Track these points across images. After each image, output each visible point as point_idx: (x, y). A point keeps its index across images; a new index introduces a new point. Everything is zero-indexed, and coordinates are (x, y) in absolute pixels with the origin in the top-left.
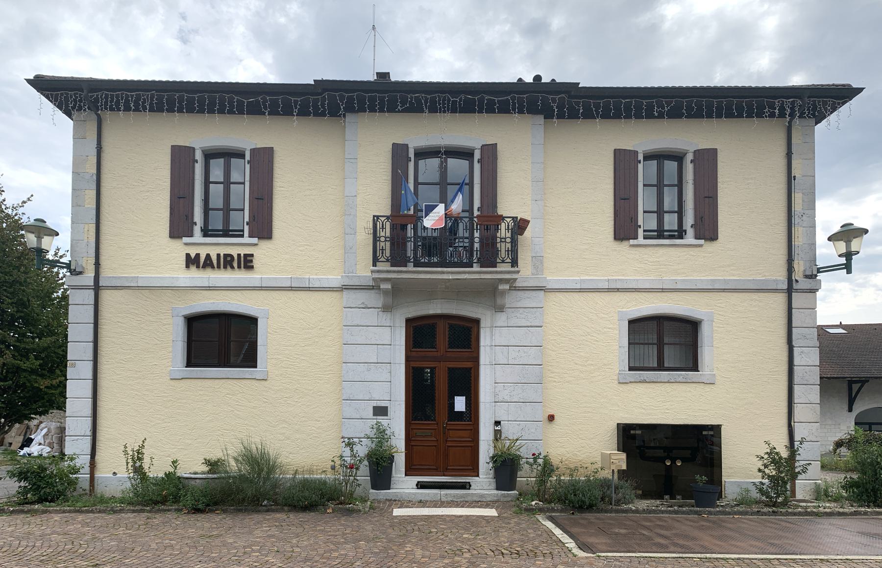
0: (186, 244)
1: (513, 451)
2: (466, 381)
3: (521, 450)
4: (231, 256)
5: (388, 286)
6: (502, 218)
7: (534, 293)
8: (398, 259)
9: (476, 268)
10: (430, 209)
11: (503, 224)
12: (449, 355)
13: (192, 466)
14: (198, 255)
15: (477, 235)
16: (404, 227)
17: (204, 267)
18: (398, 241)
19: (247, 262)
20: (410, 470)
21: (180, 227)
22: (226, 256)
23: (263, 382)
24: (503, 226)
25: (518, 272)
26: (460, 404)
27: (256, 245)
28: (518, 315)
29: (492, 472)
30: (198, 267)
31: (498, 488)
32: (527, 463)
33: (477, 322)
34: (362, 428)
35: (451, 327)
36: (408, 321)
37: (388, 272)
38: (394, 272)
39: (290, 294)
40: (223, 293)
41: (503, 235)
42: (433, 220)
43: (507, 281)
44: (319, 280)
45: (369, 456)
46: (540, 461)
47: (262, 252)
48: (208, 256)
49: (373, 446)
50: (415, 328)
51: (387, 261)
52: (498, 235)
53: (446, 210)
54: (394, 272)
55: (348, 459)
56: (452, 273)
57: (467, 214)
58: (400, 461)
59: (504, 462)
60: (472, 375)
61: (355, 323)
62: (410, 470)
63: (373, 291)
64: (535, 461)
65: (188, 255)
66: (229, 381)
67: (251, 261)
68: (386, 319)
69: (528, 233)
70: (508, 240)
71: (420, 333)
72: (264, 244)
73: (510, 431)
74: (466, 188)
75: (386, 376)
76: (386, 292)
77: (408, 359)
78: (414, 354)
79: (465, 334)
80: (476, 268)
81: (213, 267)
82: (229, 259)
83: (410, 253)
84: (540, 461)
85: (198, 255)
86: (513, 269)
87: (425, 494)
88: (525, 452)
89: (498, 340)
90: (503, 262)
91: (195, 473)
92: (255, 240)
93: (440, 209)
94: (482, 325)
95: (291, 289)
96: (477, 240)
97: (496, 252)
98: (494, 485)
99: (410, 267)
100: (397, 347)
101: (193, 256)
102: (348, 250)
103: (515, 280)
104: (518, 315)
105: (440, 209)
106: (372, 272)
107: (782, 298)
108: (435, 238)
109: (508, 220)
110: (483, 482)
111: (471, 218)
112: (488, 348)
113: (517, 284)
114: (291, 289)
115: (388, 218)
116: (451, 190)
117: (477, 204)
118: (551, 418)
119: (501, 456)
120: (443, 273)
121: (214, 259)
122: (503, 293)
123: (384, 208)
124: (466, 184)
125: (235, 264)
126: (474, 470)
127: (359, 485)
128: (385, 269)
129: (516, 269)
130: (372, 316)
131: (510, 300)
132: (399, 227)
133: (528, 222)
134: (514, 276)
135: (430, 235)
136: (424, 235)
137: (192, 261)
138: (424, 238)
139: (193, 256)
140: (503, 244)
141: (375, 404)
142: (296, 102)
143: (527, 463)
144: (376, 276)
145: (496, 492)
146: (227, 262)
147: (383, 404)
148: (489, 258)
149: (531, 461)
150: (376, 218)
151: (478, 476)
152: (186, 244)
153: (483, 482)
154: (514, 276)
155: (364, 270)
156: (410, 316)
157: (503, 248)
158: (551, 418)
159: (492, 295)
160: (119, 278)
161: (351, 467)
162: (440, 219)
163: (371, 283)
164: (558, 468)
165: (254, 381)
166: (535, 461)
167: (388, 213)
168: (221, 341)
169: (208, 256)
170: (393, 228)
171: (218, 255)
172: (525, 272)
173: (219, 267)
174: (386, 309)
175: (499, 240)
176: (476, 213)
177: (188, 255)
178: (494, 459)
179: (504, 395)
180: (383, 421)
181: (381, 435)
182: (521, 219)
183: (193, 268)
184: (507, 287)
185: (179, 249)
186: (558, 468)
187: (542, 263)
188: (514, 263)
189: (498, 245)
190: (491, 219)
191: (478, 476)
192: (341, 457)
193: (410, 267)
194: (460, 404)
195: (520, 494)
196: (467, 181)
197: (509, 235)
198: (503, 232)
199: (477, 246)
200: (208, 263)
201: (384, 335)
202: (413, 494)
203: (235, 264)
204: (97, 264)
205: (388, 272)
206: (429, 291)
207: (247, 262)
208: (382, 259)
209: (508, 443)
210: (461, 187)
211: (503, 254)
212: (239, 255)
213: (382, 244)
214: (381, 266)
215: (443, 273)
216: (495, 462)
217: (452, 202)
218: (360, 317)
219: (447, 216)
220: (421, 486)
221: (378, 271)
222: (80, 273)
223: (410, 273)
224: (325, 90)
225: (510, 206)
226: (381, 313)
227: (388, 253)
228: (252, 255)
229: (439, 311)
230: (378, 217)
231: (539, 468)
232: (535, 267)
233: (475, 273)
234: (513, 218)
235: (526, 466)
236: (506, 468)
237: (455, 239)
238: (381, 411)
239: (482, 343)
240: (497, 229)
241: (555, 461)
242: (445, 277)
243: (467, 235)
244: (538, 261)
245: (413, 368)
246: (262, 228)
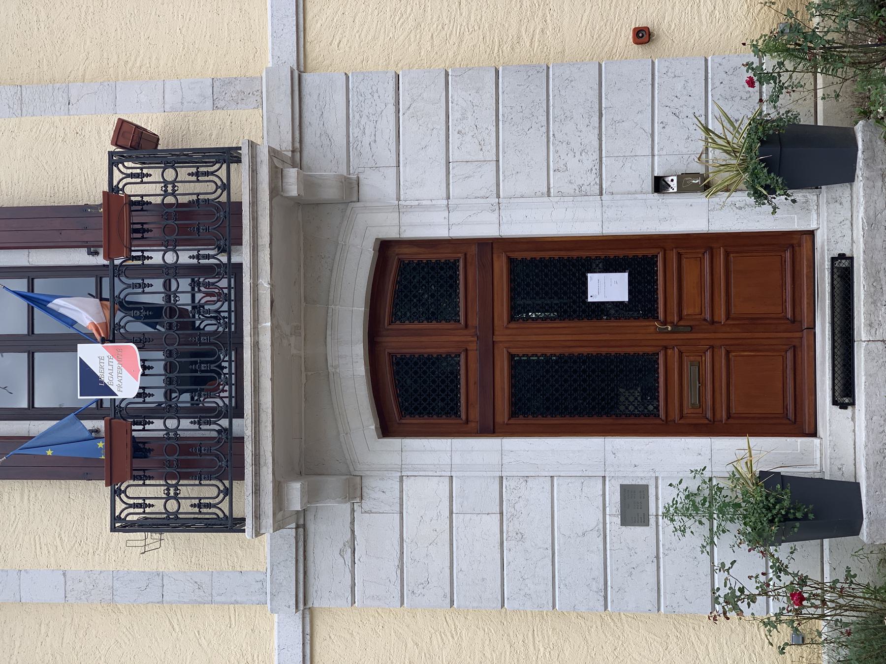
1: (738, 140)
2: (547, 271)
3: (734, 114)
5: (295, 491)
6: (112, 193)
7: (310, 101)
8: (221, 460)
9: (243, 256)
10: (90, 381)
11: (129, 190)
12: (474, 321)
15: (156, 258)
16: (140, 449)
18: (182, 461)
20: (802, 424)
24: (133, 190)
25: (252, 145)
28: (367, 140)
29: (799, 195)
31: (848, 177)
32: (774, 99)
33: (385, 248)
34: (689, 560)
35: (396, 317)
36: (386, 429)
37: (257, 491)
38: (257, 474)
41: (158, 189)
42: (123, 374)
43: (277, 175)
45: (759, 539)
46: (769, 63)
49: (735, 527)
50: (407, 410)
51: (228, 492)
52: (158, 200)
53: (89, 338)
54: (257, 474)
56: (256, 320)
57: (106, 282)
58: (774, 452)
59: (771, 165)
60: (528, 255)
62: (802, 424)
63: (311, 527)
64: (769, 77)
68: (381, 491)
69: (151, 123)
70: (170, 174)
71: (418, 397)
73: (680, 152)
74: (42, 286)
75: (537, 492)
76: (312, 495)
77: (489, 429)
78: (475, 414)
79: (417, 279)
80: (243, 256)
83: (210, 431)
84: (769, 63)
86: (245, 159)
88: (743, 107)
89: (433, 189)
90: (226, 187)
93: (92, 354)
94: (392, 234)
96: (170, 258)
97: (198, 205)
98: (840, 190)
99: (243, 426)
100: (457, 460)
102: (205, 594)
103: (274, 153)
104: (367, 140)
105: (92, 354)
106: (258, 533)
108: (169, 367)
109: (117, 176)
110: (829, 220)
111: (117, 272)
112: (455, 217)
113: (285, 144)
115: (116, 493)
116: (44, 325)
117: (79, 257)
118: (643, 36)
119: (754, 175)
120: (256, 346)
122: (308, 183)
123: (86, 503)
124: (31, 287)
126: (798, 243)
128: (249, 499)
129: (245, 153)
130: (375, 528)
131: (327, 164)
132: (139, 463)
133: (122, 123)
134: (264, 156)
135: (160, 381)
136: (159, 396)
138: (168, 395)
140: (181, 188)
143: (774, 99)
144: (268, 521)
145: (859, 184)
148: (217, 223)
149: (767, 89)
150: (119, 525)
151: (811, 233)
153: (829, 220)
154: (264, 156)
155: (257, 552)
156: (374, 433)
157: (190, 187)
158: (643, 36)
159: (312, 213)
162: (116, 355)
163: (289, 532)
166: (769, 77)
167: (100, 490)
170: (142, 476)
172: (253, 126)
174: (354, 490)
175: (170, 200)
176: (100, 260)
178: (762, 193)
179: (580, 169)
180: (662, 497)
181: (703, 504)
182: (115, 142)
184: (292, 174)
187: (229, 82)
188: (229, 156)
189: (183, 200)
190: (117, 222)
191: (811, 233)
193: (243, 426)
194: (608, 287)
196: (21, 285)
197: (156, 174)
198: (148, 187)
199: (185, 257)
201: (425, 496)
205: (257, 491)
206: (304, 380)
208: (225, 506)
209: (716, 155)
210: (36, 302)
211: (206, 188)
213: (186, 506)
214: (243, 506)
215: (256, 346)
216: (772, 191)
217: (71, 323)
219: (111, 335)
220: (845, 395)
221: (257, 517)
223: (259, 427)
225: (80, 172)
226: (367, 504)
227: (208, 491)
230: (115, 519)
231: (789, 65)
232: (240, 99)
233: (257, 257)
234: (112, 164)
235: (784, 100)
236: (787, 156)
237: (172, 311)
239: (441, 232)
240: (142, 205)
241: (767, 23)
242: (266, 340)
243: (158, 284)
244: (224, 91)
245: (513, 414)
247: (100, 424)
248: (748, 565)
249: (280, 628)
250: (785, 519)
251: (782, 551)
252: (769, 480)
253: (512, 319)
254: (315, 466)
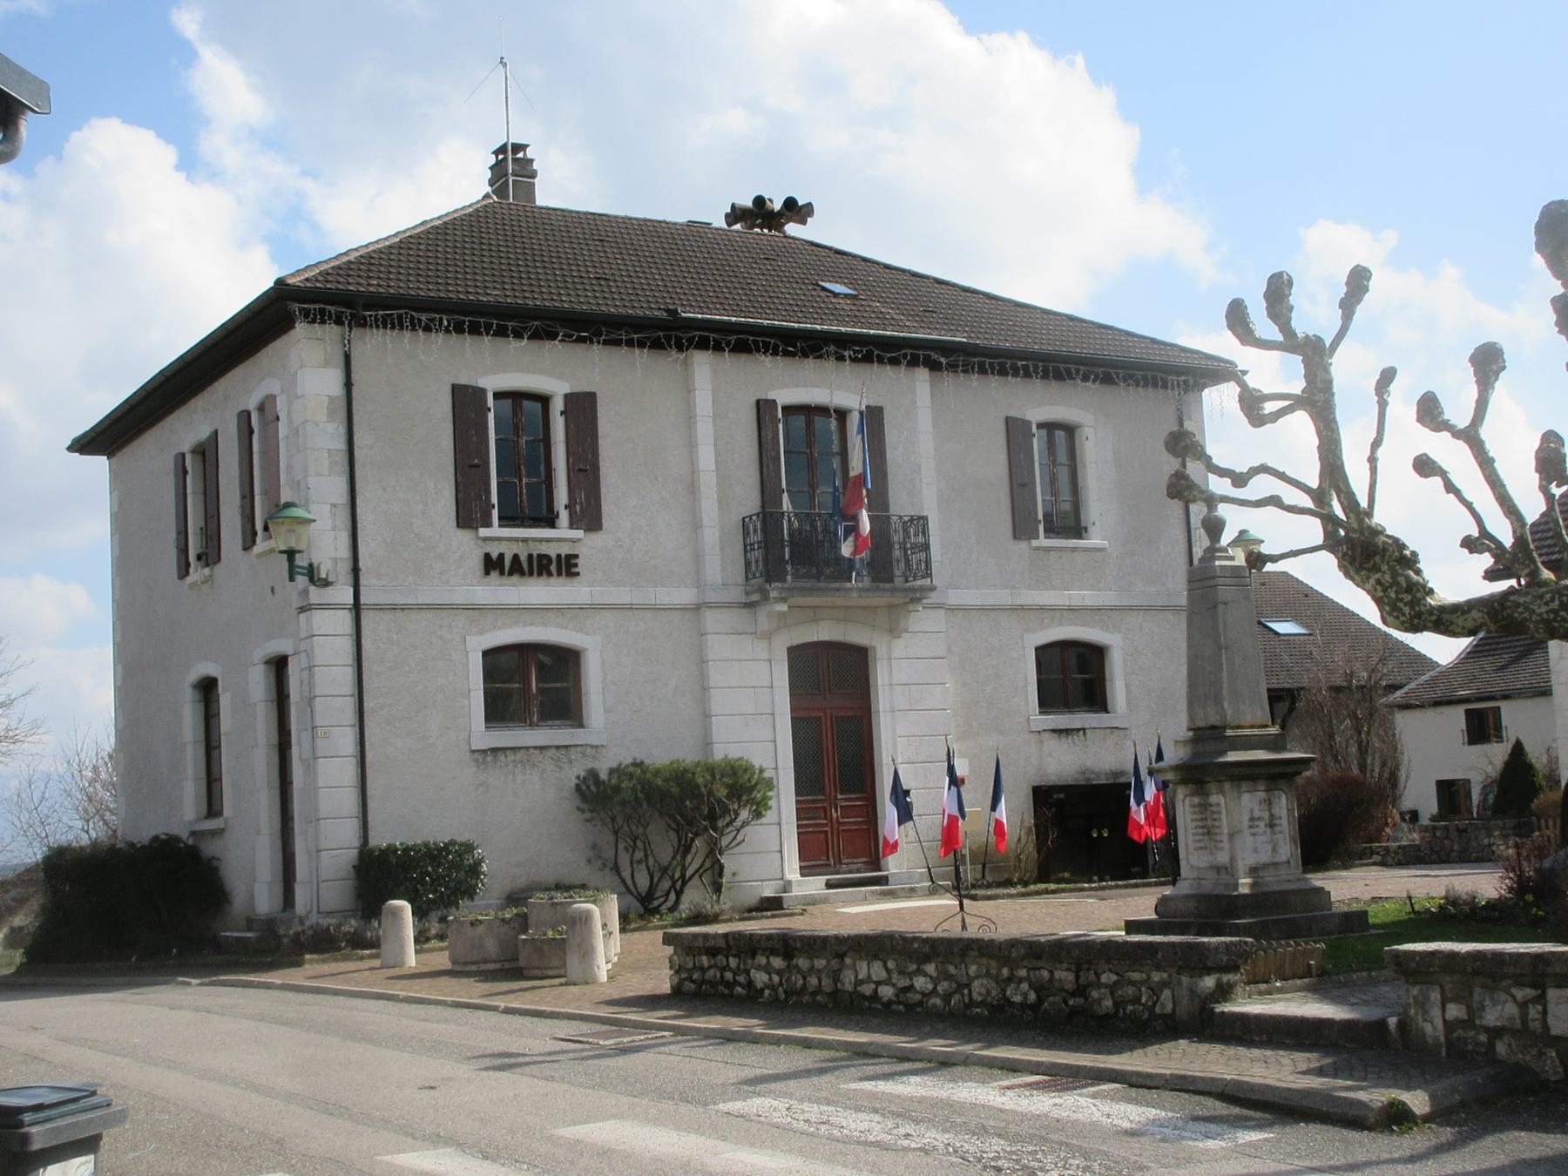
4: (548, 557)
14: (501, 556)
17: (511, 574)
19: (567, 566)
21: (469, 514)
22: (540, 557)
30: (502, 573)
36: (792, 651)
40: (533, 612)
47: (588, 546)
48: (516, 557)
65: (487, 556)
67: (576, 565)
72: (595, 539)
81: (522, 574)
85: (501, 556)
92: (579, 534)
101: (494, 555)
121: (523, 558)
125: (553, 568)
137: (492, 565)
139: (494, 555)
146: (541, 566)
169: (516, 557)
173: (531, 574)
177: (487, 556)
183: (494, 574)
185: (467, 547)
203: (553, 568)
228: (576, 556)
246: (589, 516)
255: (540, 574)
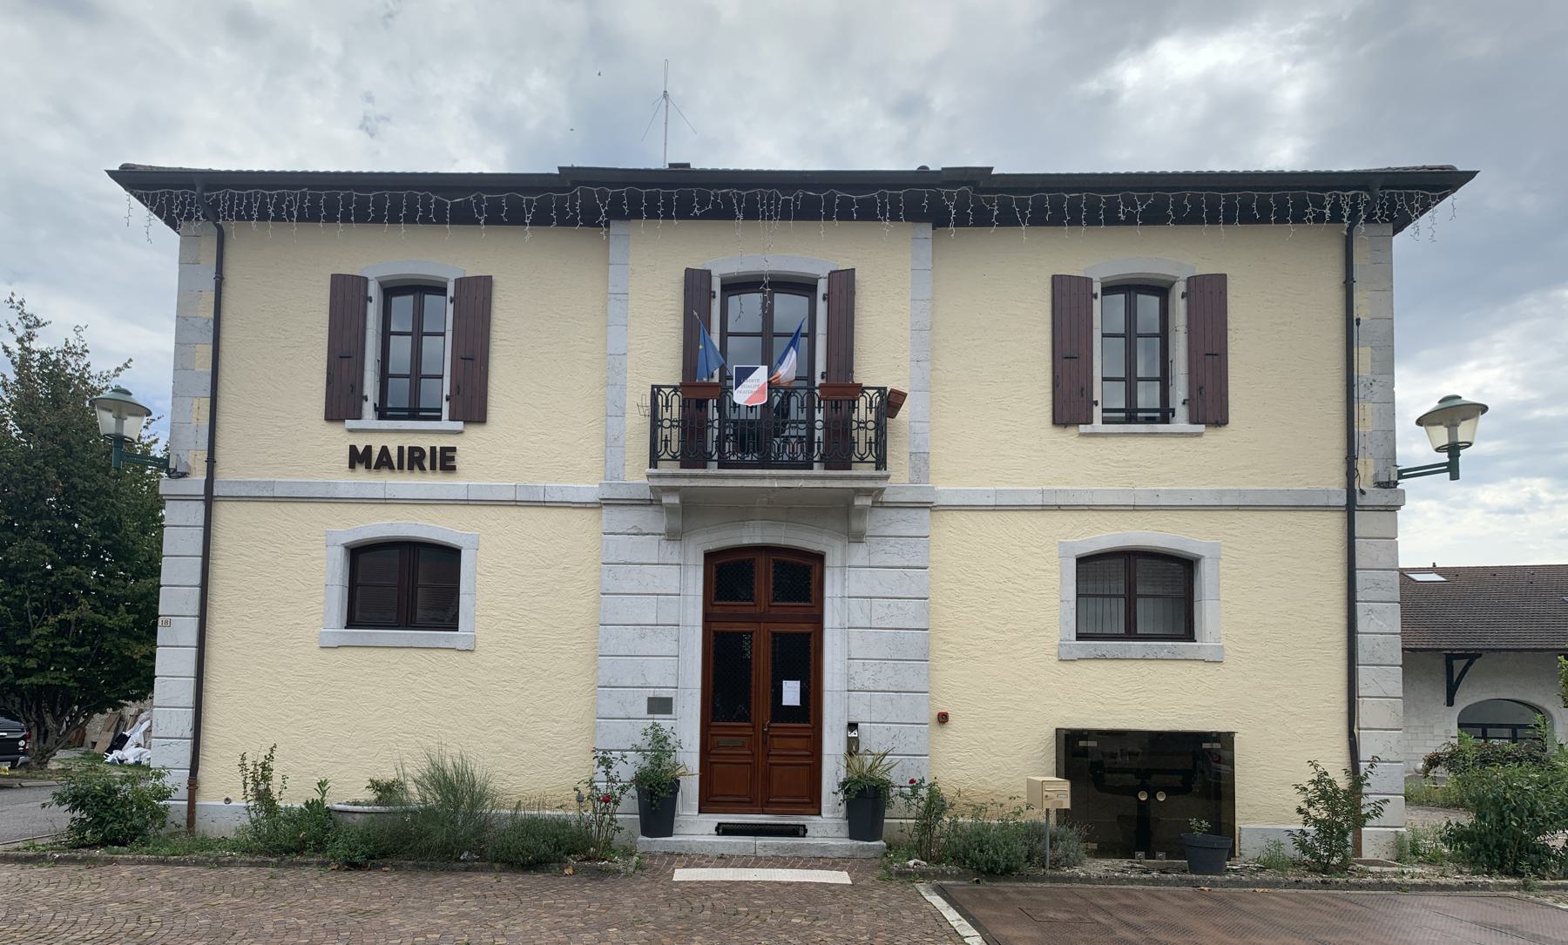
0: (351, 431)
1: (878, 774)
2: (802, 655)
3: (892, 771)
5: (674, 500)
6: (861, 389)
8: (693, 456)
9: (818, 470)
10: (744, 374)
11: (862, 400)
12: (773, 611)
13: (350, 790)
14: (368, 449)
15: (819, 416)
16: (702, 404)
17: (377, 467)
18: (692, 427)
19: (445, 461)
20: (706, 806)
21: (341, 403)
23: (468, 655)
24: (862, 402)
25: (887, 478)
26: (791, 693)
27: (461, 432)
28: (887, 548)
29: (843, 807)
30: (368, 467)
31: (852, 836)
32: (901, 794)
33: (820, 558)
34: (628, 734)
35: (780, 566)
36: (709, 556)
37: (674, 476)
38: (685, 476)
39: (513, 511)
40: (406, 511)
41: (862, 417)
42: (749, 393)
43: (868, 492)
44: (561, 490)
45: (640, 780)
46: (923, 792)
47: (470, 443)
48: (384, 450)
49: (646, 764)
50: (720, 568)
51: (674, 458)
52: (855, 417)
53: (770, 374)
54: (685, 476)
55: (602, 786)
57: (804, 383)
58: (690, 788)
59: (862, 792)
60: (812, 646)
61: (622, 559)
62: (706, 806)
63: (650, 509)
64: (915, 793)
65: (353, 449)
66: (413, 653)
67: (453, 459)
68: (672, 552)
69: (903, 414)
70: (871, 425)
71: (727, 576)
72: (474, 432)
73: (873, 739)
74: (804, 342)
75: (669, 646)
76: (670, 510)
77: (708, 618)
78: (717, 610)
79: (800, 577)
80: (818, 470)
81: (391, 468)
82: (417, 454)
83: (711, 447)
84: (923, 792)
85: (368, 449)
86: (878, 473)
87: (730, 844)
88: (898, 777)
89: (855, 588)
90: (862, 460)
91: (356, 804)
92: (459, 425)
93: (761, 375)
94: (828, 562)
95: (515, 503)
96: (819, 425)
97: (850, 444)
98: (845, 831)
99: (713, 469)
100: (690, 599)
101: (361, 449)
102: (611, 443)
103: (882, 490)
104: (887, 548)
105: (761, 375)
106: (649, 476)
107: (1336, 521)
108: (751, 423)
109: (871, 392)
110: (827, 826)
111: (811, 391)
112: (837, 602)
113: (886, 498)
114: (515, 503)
115: (675, 389)
116: (779, 344)
117: (820, 366)
118: (943, 718)
119: (857, 782)
120: (763, 477)
122: (862, 511)
123: (670, 372)
124: (804, 335)
125: (427, 464)
126: (815, 807)
127: (619, 829)
128: (670, 472)
129: (883, 473)
130: (650, 548)
131: (874, 523)
132: (693, 404)
133: (905, 395)
134: (880, 484)
135: (743, 417)
136: (734, 417)
137: (358, 458)
138: (735, 422)
139: (361, 449)
140: (862, 432)
141: (651, 693)
142: (529, 203)
143: (901, 794)
144: (656, 482)
145: (849, 842)
146: (414, 460)
147: (664, 693)
148: (839, 453)
149: (908, 791)
150: (656, 390)
151: (819, 814)
152: (351, 431)
153: (827, 826)
154: (880, 484)
155: (636, 474)
156: (711, 547)
157: (862, 438)
158: (943, 718)
159: (843, 514)
160: (245, 483)
161: (607, 799)
162: (760, 390)
163: (648, 495)
164: (952, 805)
165: (453, 653)
166: (915, 793)
167: (677, 380)
168: (403, 587)
169: (384, 450)
170: (684, 405)
171: (401, 449)
172: (899, 477)
173: (401, 467)
174: (673, 535)
175: (855, 425)
176: (818, 381)
177: (353, 449)
178: (846, 786)
179: (864, 678)
180: (664, 722)
181: (660, 746)
182: (892, 391)
183: (361, 469)
184: (869, 502)
185: (339, 439)
186: (952, 805)
187: (926, 463)
188: (881, 462)
189: (854, 433)
190: (843, 391)
191: (819, 814)
192: (591, 782)
193: (713, 469)
194: (791, 693)
195: (889, 847)
196: (805, 330)
197: (871, 417)
198: (863, 411)
199: (819, 434)
200: (384, 461)
201: (669, 578)
202: (710, 844)
203: (427, 464)
204: (211, 461)
205: (674, 476)
206: (740, 507)
207: (445, 461)
208: (666, 456)
209: (869, 760)
210: (794, 339)
211: (861, 447)
212: (433, 449)
213: (666, 432)
214: (666, 468)
215: (763, 477)
216: (846, 792)
217: (780, 362)
218: (627, 547)
219: (772, 386)
220: (723, 830)
221: (659, 476)
222: (184, 475)
223: (712, 478)
224: (576, 183)
225: (874, 368)
226: (664, 543)
227: (675, 446)
228: (454, 449)
229: (758, 540)
230: (659, 387)
231: (922, 804)
232: (916, 470)
233: (817, 478)
234: (879, 389)
235: (900, 801)
236: (867, 802)
237: (784, 425)
238: (661, 705)
239: (828, 592)
240: (853, 408)
241: (948, 791)
242: (766, 484)
243: (803, 417)
244: (921, 461)
245: (716, 633)
247: (716, 379)
248: (626, 771)
249: (590, 488)
250: (652, 794)
251: (633, 791)
252: (675, 786)
253: (774, 634)
254: (688, 512)
255: (411, 468)
